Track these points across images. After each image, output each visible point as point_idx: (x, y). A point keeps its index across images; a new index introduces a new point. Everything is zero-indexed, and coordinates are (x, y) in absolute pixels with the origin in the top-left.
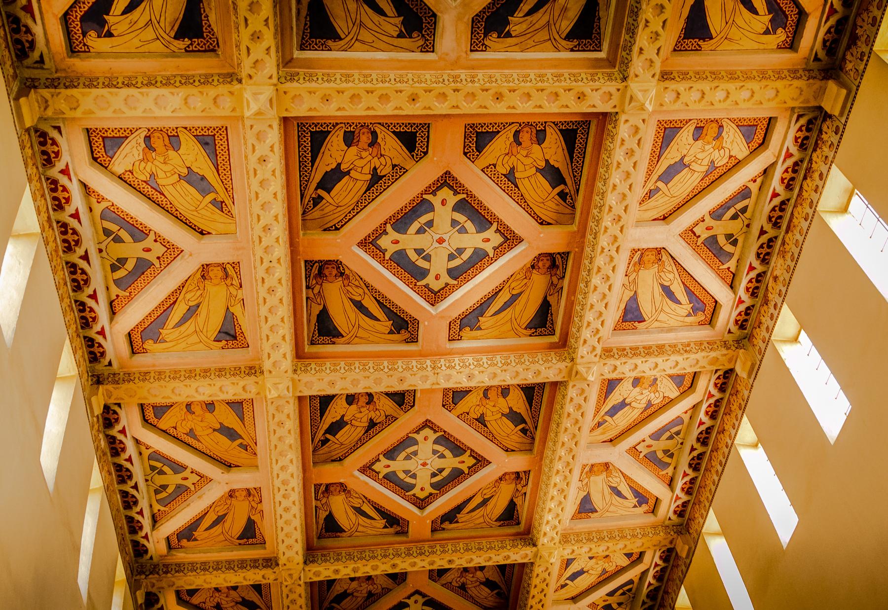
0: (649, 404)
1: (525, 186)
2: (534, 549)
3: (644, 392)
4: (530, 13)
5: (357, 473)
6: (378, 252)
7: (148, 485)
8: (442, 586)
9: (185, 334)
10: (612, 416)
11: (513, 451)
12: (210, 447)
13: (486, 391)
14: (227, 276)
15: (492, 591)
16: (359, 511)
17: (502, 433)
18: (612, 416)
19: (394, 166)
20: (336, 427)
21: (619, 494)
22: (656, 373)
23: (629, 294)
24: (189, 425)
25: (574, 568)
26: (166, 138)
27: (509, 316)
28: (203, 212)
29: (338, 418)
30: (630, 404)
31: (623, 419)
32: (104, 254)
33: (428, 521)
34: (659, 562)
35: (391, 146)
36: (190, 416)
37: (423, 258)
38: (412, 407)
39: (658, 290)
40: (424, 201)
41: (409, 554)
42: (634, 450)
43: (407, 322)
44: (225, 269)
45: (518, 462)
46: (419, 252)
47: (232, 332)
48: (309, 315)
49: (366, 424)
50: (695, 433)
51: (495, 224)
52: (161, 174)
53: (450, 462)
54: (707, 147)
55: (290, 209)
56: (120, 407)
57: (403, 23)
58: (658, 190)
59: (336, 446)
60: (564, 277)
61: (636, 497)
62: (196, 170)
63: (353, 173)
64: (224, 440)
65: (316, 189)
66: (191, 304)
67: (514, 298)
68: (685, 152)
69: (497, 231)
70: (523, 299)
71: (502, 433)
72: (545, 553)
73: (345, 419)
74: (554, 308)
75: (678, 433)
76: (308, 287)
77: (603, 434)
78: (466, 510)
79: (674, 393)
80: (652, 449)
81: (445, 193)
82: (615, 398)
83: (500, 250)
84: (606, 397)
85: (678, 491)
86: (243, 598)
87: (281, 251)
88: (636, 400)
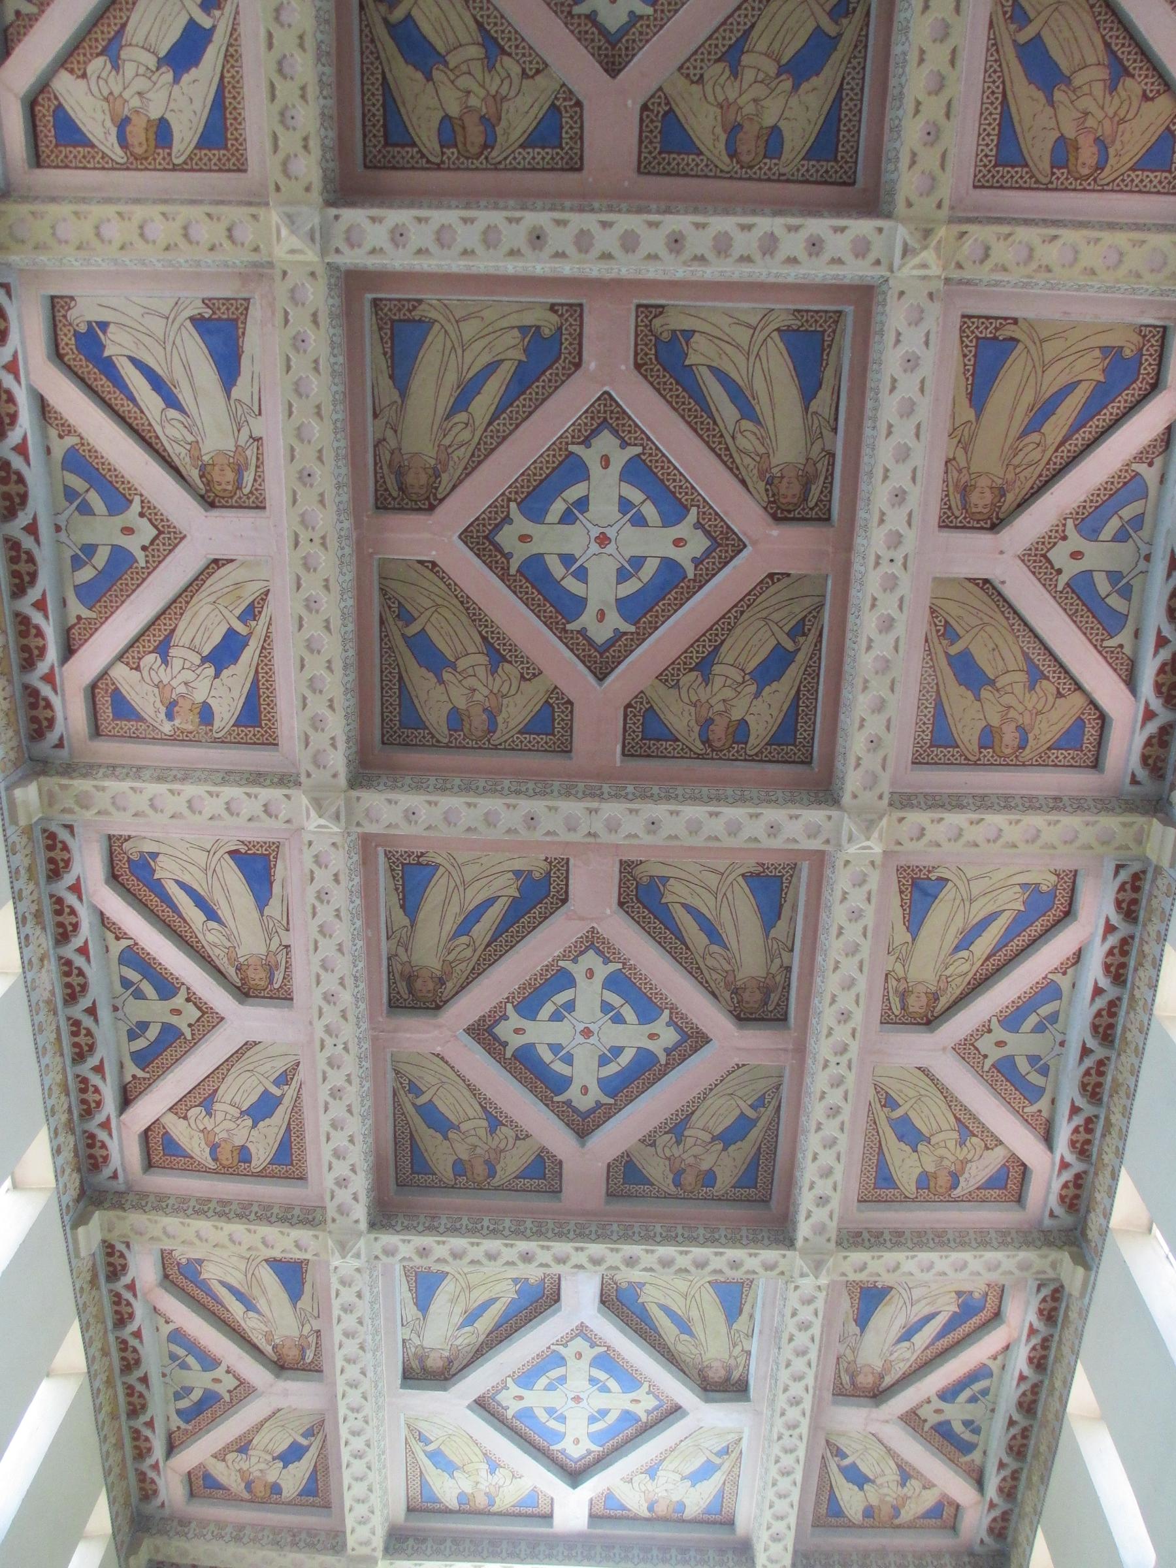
1: (472, 1108)
4: (493, 1301)
6: (678, 1021)
7: (1150, 544)
9: (989, 896)
10: (231, 633)
12: (1010, 638)
14: (903, 995)
15: (409, 17)
19: (653, 1145)
23: (274, 909)
24: (1031, 701)
26: (932, 1184)
27: (470, 893)
28: (911, 1093)
29: (767, 689)
32: (1059, 1038)
33: (593, 366)
35: (656, 1170)
36: (1027, 721)
37: (613, 1008)
38: (629, 705)
39: (224, 912)
40: (613, 1095)
43: (639, 901)
44: (903, 1008)
46: (618, 1019)
47: (916, 895)
48: (792, 920)
49: (717, 669)
51: (509, 1055)
52: (951, 1144)
54: (224, 1135)
55: (798, 1105)
56: (1133, 775)
57: (639, 1296)
58: (277, 1082)
59: (776, 617)
60: (389, 959)
62: (908, 1149)
63: (708, 1137)
64: (983, 658)
65: (759, 1118)
66: (965, 954)
67: (465, 927)
68: (254, 1132)
69: (505, 1044)
70: (450, 926)
72: (311, 256)
73: (753, 688)
74: (395, 900)
76: (789, 969)
78: (505, 372)
80: (119, 521)
81: (584, 1103)
82: (239, 676)
83: (497, 1016)
84: (255, 683)
87: (822, 1048)
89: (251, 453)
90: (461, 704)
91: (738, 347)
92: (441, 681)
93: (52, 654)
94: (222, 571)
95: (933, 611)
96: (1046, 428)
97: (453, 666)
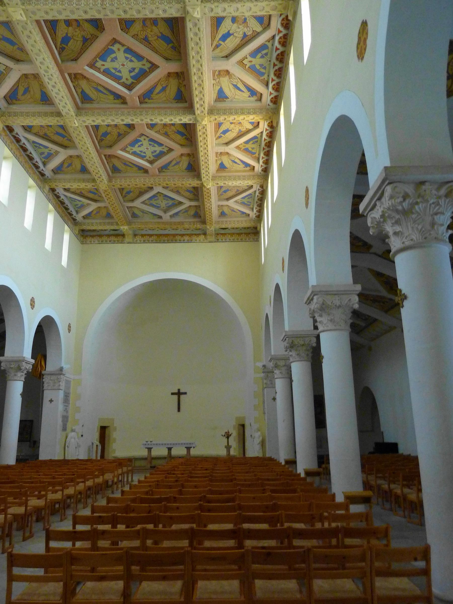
0: (245, 35)
2: (194, 116)
3: (240, 27)
5: (87, 68)
8: (155, 132)
10: (224, 41)
11: (170, 60)
13: (144, 20)
16: (97, 89)
17: (161, 49)
18: (224, 41)
20: (66, 40)
21: (239, 89)
22: (247, 14)
25: (223, 128)
30: (233, 34)
31: (231, 43)
34: (268, 128)
41: (129, 115)
42: (241, 63)
45: (173, 67)
50: (275, 55)
53: (137, 65)
61: (249, 91)
71: (161, 49)
72: (199, 119)
73: (69, 35)
75: (266, 54)
77: (221, 52)
79: (259, 28)
80: (253, 63)
82: (223, 30)
84: (217, 29)
85: (270, 89)
86: (56, 131)
88: (236, 32)
89: (216, 77)
90: (154, 28)
91: (103, 98)
92: (161, 33)
93: (277, 38)
94: (225, 55)
95: (28, 54)
96: (23, 89)
97: (158, 37)
